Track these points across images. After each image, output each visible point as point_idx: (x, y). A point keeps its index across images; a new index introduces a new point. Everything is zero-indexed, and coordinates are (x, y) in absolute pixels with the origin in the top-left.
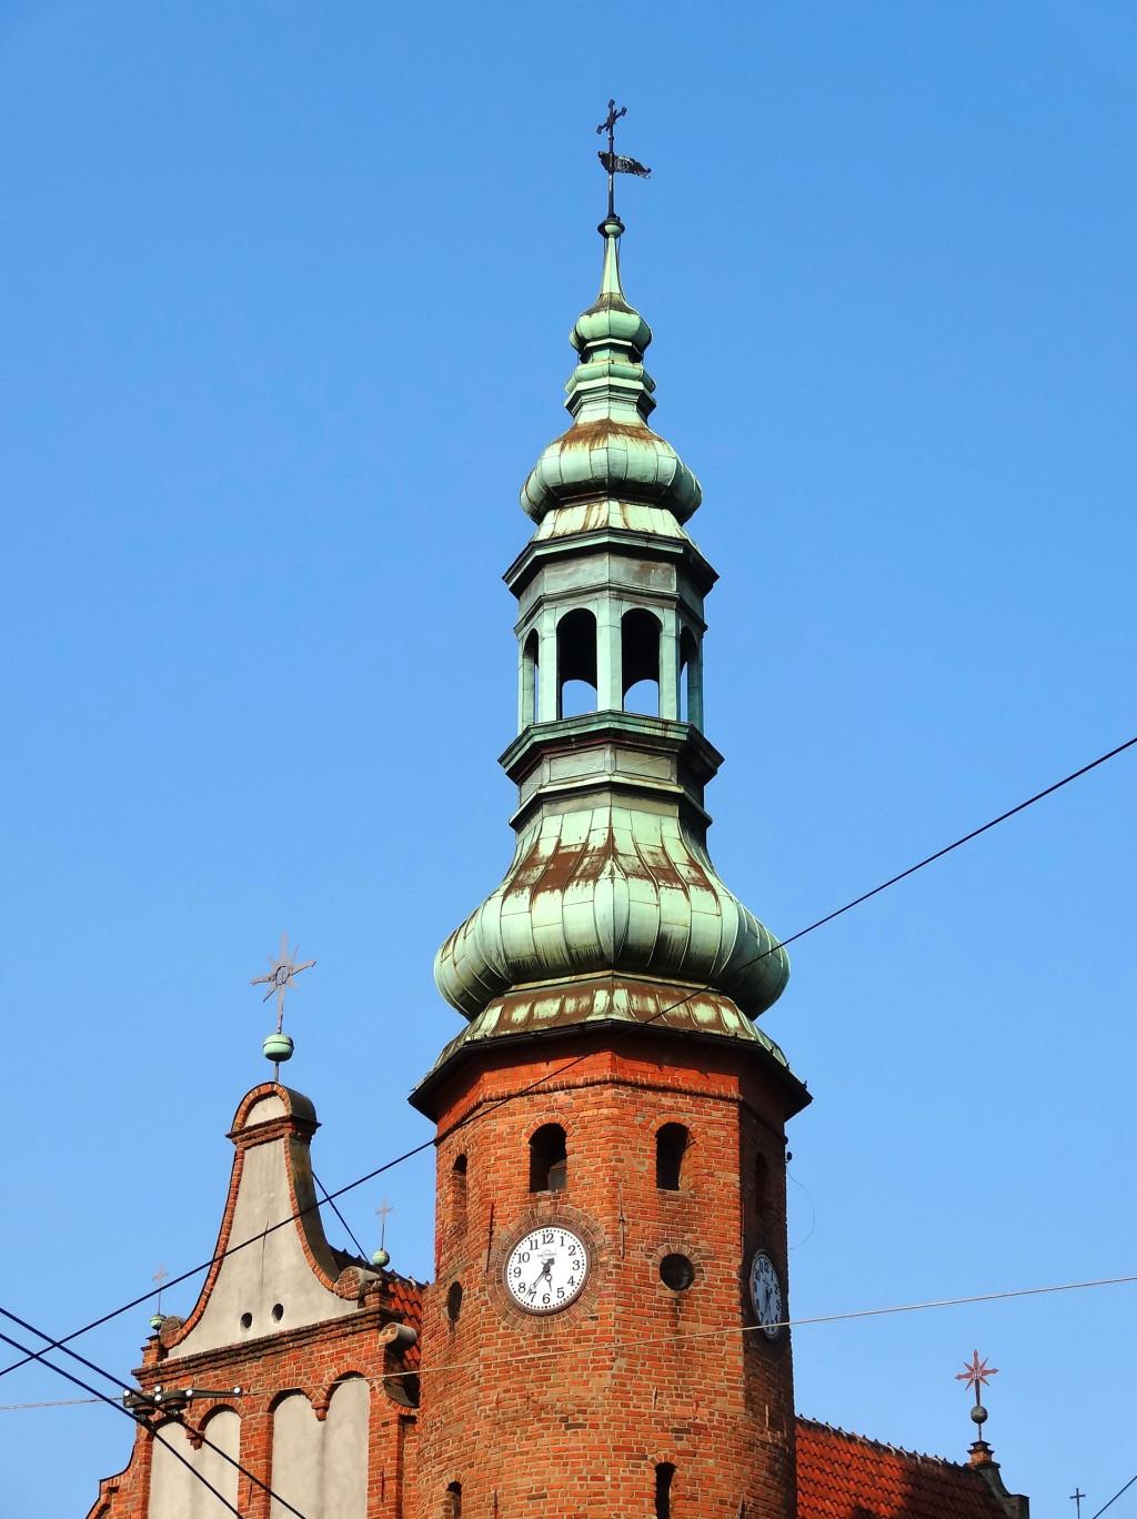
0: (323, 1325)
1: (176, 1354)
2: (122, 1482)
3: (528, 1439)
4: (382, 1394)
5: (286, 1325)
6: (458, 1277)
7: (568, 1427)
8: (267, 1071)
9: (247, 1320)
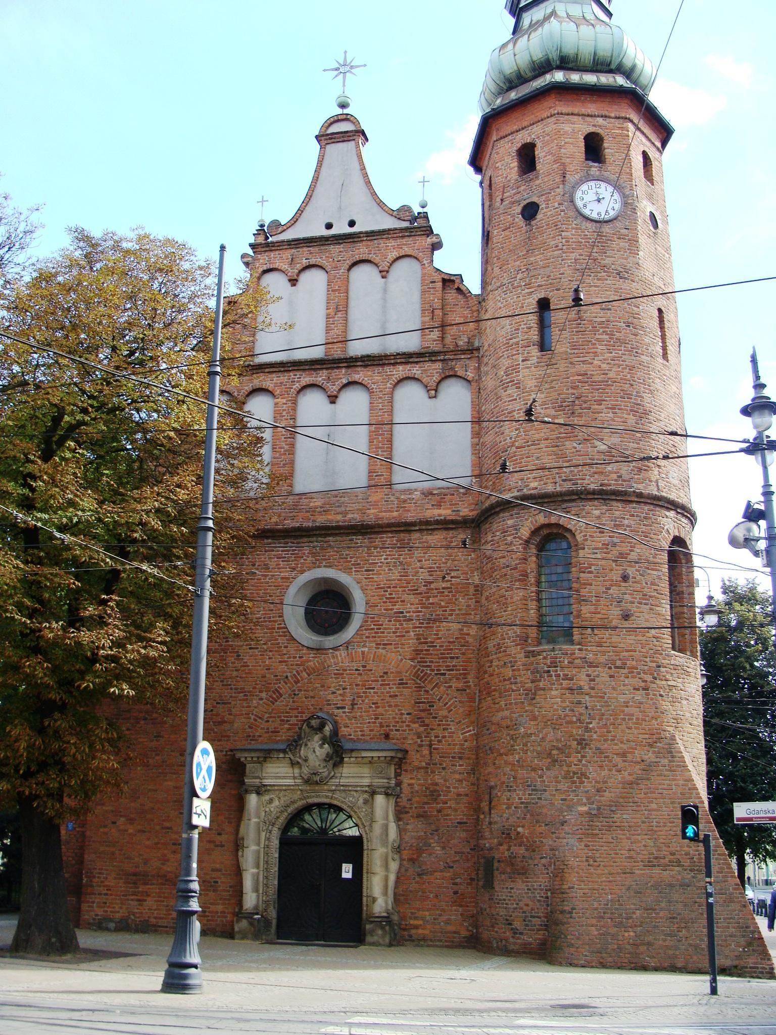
0: (389, 230)
3: (598, 280)
7: (621, 278)
8: (340, 111)
9: (329, 226)
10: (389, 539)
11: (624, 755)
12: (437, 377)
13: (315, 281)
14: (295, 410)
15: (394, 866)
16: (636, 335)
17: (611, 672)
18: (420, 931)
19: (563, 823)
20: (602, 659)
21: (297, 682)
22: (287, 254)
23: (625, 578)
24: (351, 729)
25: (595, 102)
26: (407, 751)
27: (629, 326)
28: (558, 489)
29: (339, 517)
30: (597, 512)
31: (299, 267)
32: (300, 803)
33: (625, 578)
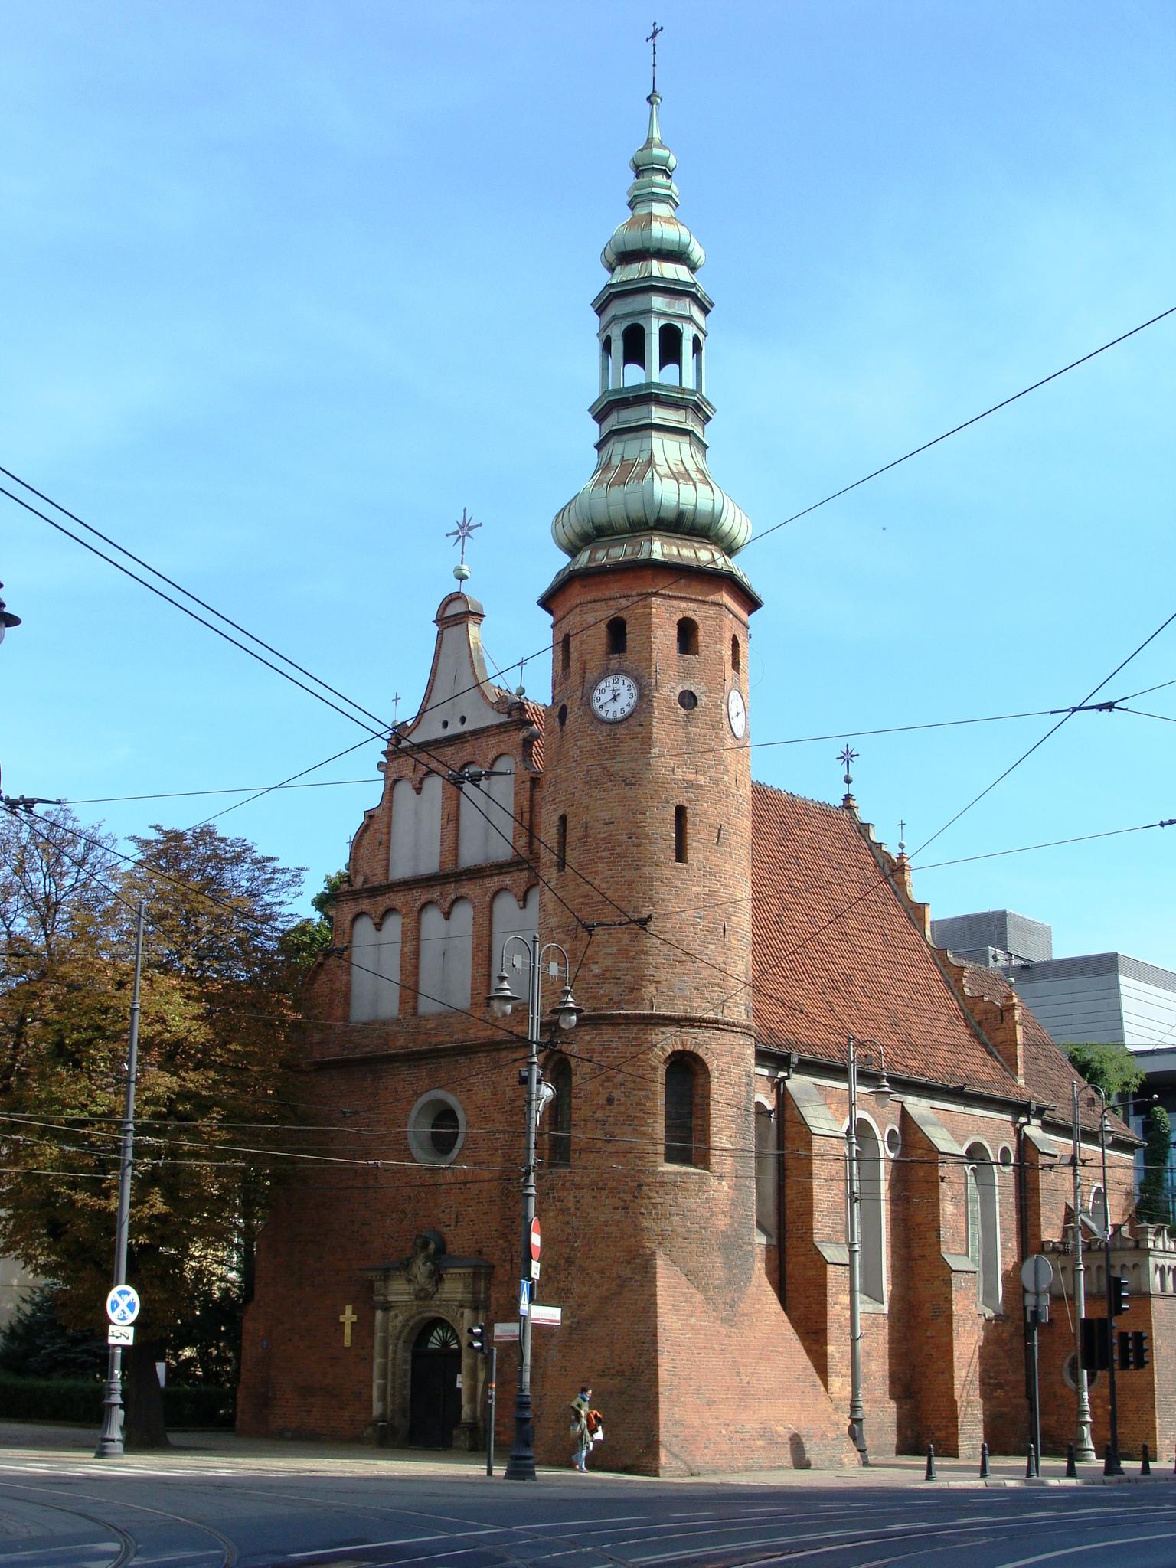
1: (404, 744)
2: (377, 813)
4: (521, 767)
6: (565, 702)
8: (454, 586)
9: (445, 724)
10: (483, 1060)
11: (601, 1272)
12: (523, 888)
14: (418, 929)
16: (638, 846)
20: (587, 1181)
21: (418, 1202)
23: (610, 1101)
25: (618, 581)
29: (447, 1039)
30: (588, 1038)
31: (420, 774)
32: (417, 1318)
33: (610, 1101)
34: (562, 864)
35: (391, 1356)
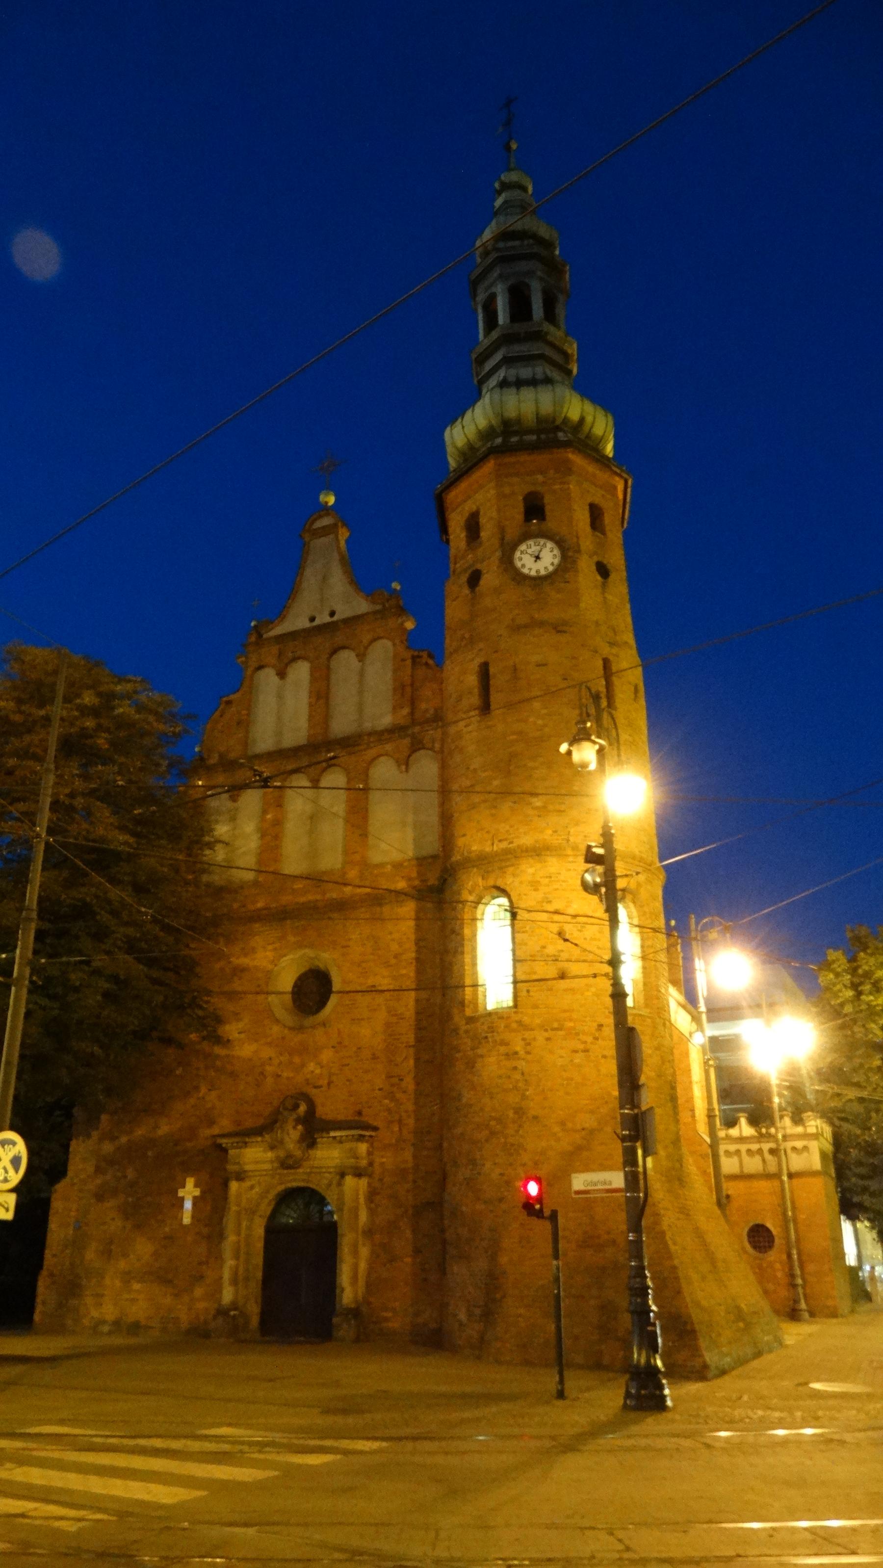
5: (335, 618)
9: (312, 619)
11: (563, 1124)
13: (301, 671)
15: (364, 1252)
17: (546, 1035)
18: (390, 1325)
19: (501, 1200)
20: (538, 1021)
22: (275, 649)
24: (327, 1109)
26: (375, 1129)
27: (566, 679)
28: (495, 848)
31: (286, 661)
34: (485, 708)
35: (243, 1233)
